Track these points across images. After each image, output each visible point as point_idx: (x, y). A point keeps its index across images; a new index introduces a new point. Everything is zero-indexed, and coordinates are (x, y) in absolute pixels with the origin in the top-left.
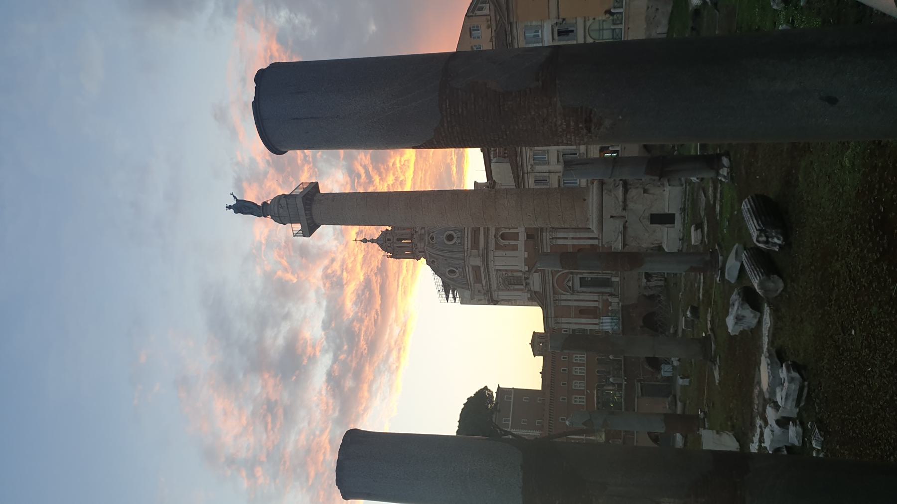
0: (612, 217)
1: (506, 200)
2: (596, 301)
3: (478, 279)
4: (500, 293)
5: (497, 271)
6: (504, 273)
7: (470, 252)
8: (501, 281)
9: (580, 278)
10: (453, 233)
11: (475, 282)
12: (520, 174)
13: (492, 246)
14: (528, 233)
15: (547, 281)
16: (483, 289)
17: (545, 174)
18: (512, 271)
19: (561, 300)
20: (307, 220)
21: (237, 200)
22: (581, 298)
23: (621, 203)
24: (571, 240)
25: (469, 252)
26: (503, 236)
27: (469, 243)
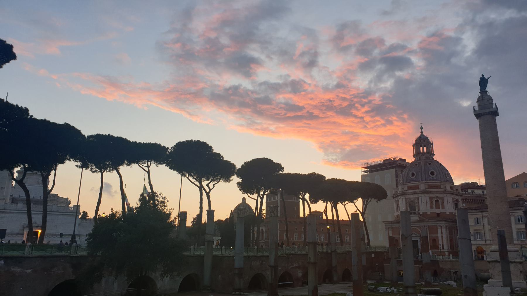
3: (410, 188)
4: (404, 200)
5: (418, 198)
6: (417, 202)
8: (411, 200)
10: (435, 175)
11: (408, 187)
14: (440, 214)
16: (405, 191)
17: (482, 223)
18: (419, 206)
20: (484, 113)
21: (488, 79)
23: (514, 260)
26: (437, 201)
27: (431, 184)
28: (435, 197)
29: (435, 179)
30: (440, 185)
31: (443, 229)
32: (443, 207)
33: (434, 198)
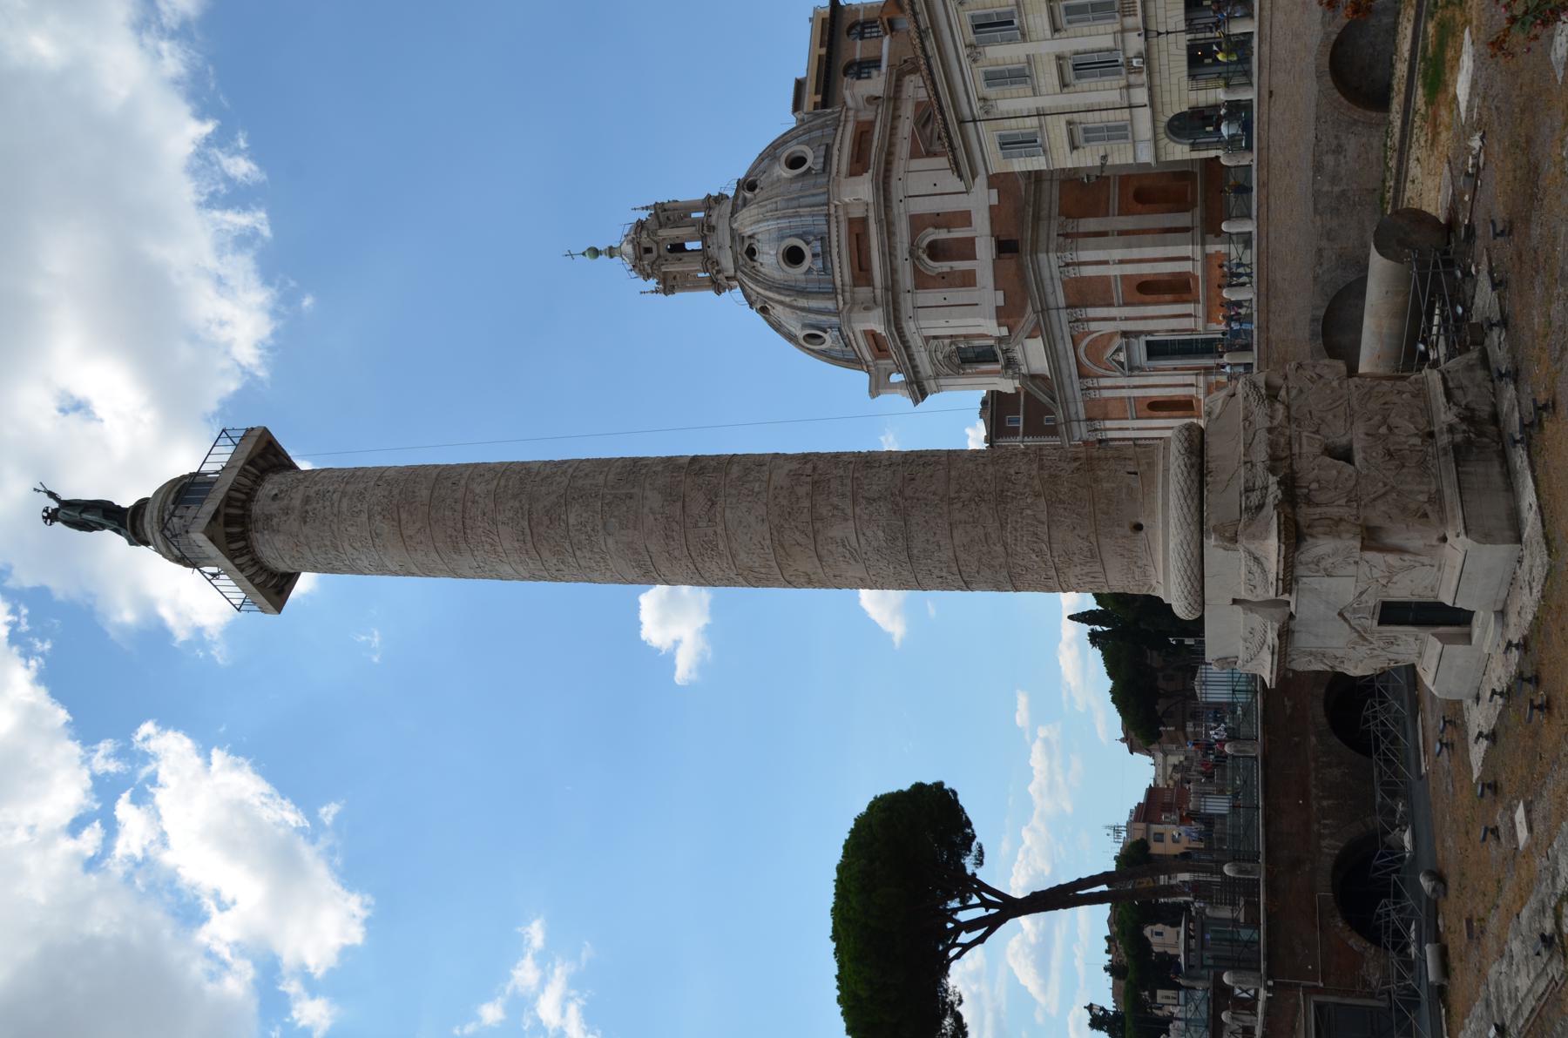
0: (1235, 601)
1: (851, 524)
2: (1192, 385)
5: (927, 339)
6: (947, 341)
7: (853, 293)
9: (1148, 343)
11: (877, 358)
12: (954, 127)
13: (906, 278)
14: (1002, 238)
15: (1061, 353)
19: (1100, 388)
22: (1151, 381)
24: (1118, 266)
25: (847, 295)
26: (937, 251)
28: (915, 266)
29: (819, 243)
30: (851, 221)
31: (1083, 260)
32: (964, 218)
33: (921, 268)
